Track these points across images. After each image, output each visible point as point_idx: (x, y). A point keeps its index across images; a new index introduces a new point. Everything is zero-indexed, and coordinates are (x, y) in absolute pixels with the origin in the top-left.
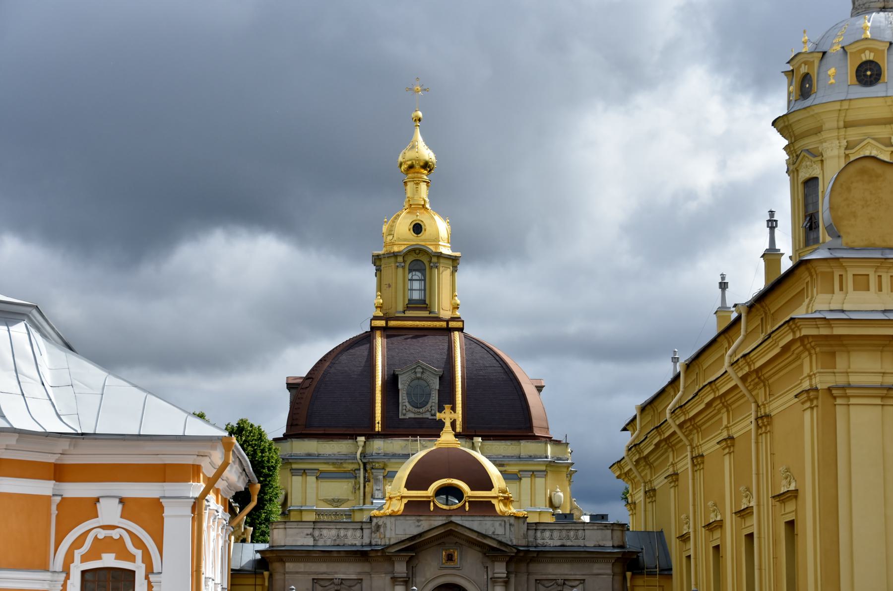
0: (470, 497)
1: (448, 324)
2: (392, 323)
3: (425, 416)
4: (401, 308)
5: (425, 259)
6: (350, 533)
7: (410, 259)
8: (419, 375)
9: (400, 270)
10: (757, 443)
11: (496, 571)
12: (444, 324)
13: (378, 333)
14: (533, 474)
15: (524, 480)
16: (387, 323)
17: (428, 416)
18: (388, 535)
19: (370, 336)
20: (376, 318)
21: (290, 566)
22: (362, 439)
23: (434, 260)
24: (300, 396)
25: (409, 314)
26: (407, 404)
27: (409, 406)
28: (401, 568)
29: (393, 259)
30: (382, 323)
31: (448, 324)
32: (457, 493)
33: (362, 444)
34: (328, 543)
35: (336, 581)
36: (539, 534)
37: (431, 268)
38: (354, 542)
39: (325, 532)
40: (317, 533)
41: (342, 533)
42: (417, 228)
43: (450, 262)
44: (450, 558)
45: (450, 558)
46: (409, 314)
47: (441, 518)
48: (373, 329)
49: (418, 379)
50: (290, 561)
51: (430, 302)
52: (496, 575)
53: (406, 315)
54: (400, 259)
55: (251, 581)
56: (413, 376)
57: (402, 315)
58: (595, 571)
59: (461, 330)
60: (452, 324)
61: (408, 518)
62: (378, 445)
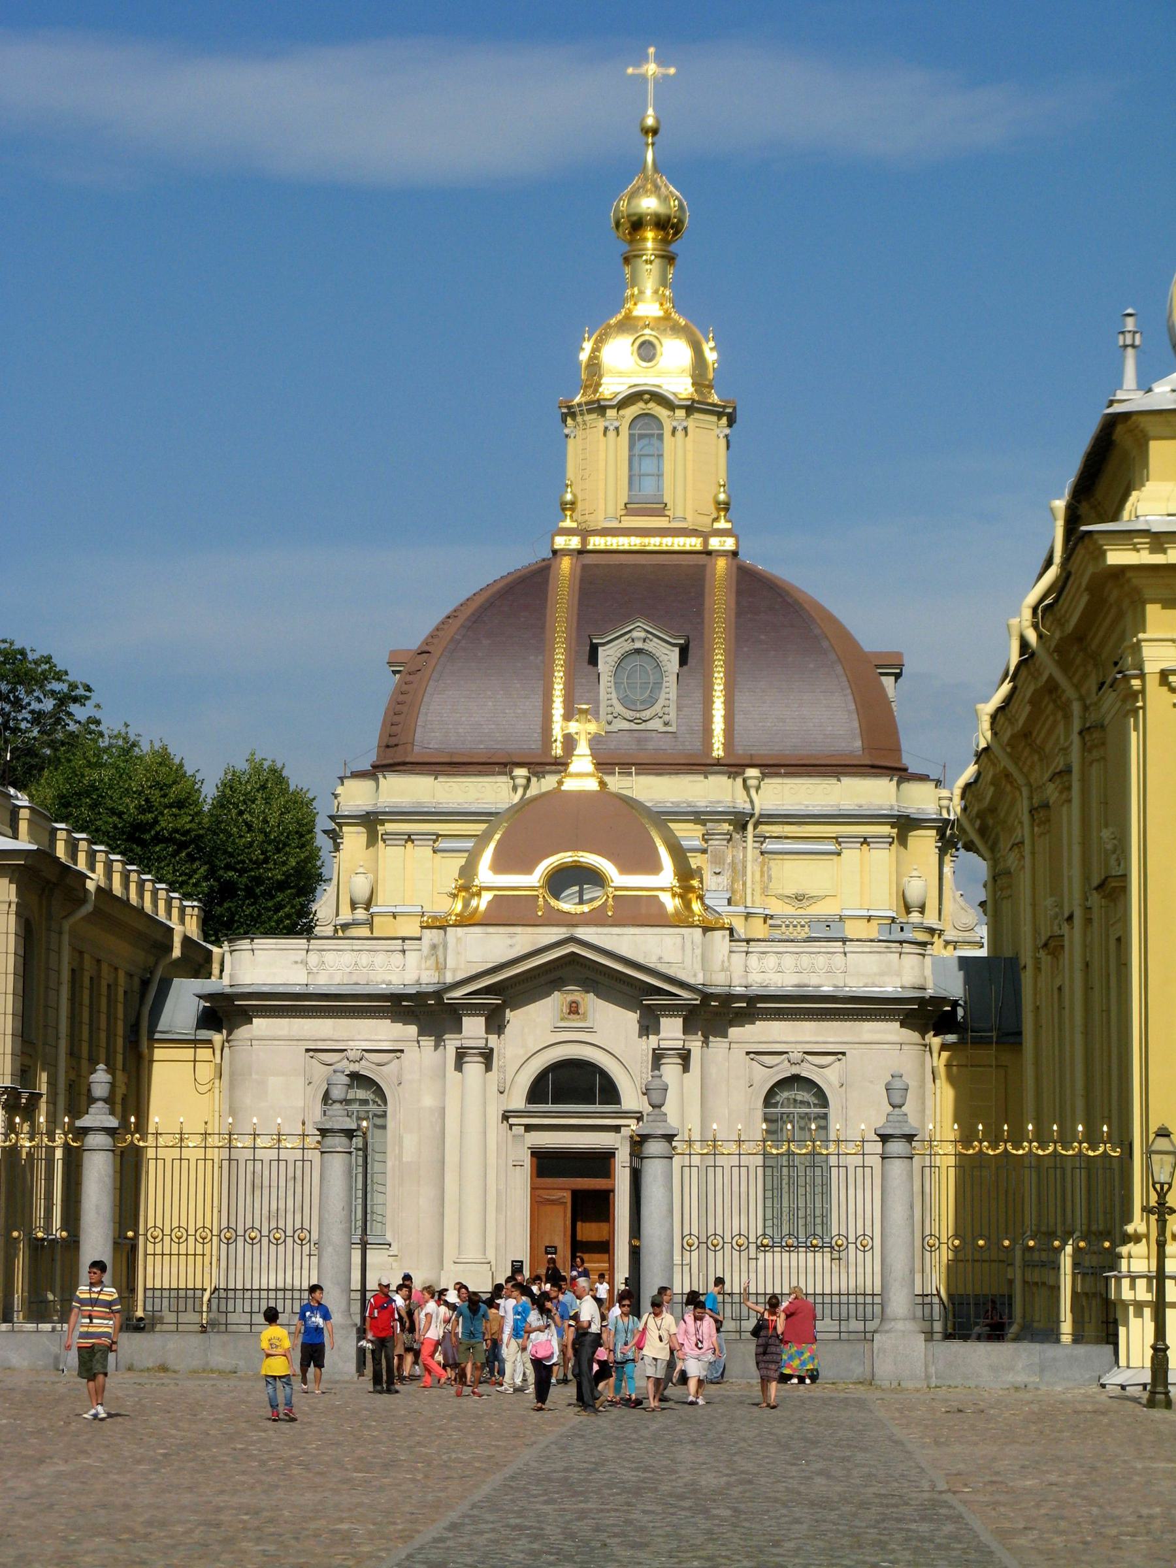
0: (617, 888)
1: (706, 543)
2: (596, 542)
3: (650, 725)
6: (380, 959)
8: (638, 645)
10: (1084, 780)
11: (663, 1035)
14: (865, 841)
16: (584, 542)
17: (656, 724)
18: (450, 963)
19: (548, 567)
21: (260, 1025)
23: (681, 413)
24: (405, 688)
26: (615, 702)
27: (619, 708)
28: (474, 1027)
30: (575, 543)
31: (706, 543)
32: (595, 878)
34: (337, 980)
35: (350, 1054)
36: (753, 960)
38: (388, 978)
39: (329, 957)
40: (313, 958)
41: (364, 959)
44: (574, 1009)
45: (574, 1009)
47: (555, 930)
49: (639, 651)
50: (260, 1017)
52: (664, 1044)
53: (624, 525)
55: (188, 1053)
56: (629, 646)
57: (615, 524)
58: (867, 1037)
61: (491, 929)
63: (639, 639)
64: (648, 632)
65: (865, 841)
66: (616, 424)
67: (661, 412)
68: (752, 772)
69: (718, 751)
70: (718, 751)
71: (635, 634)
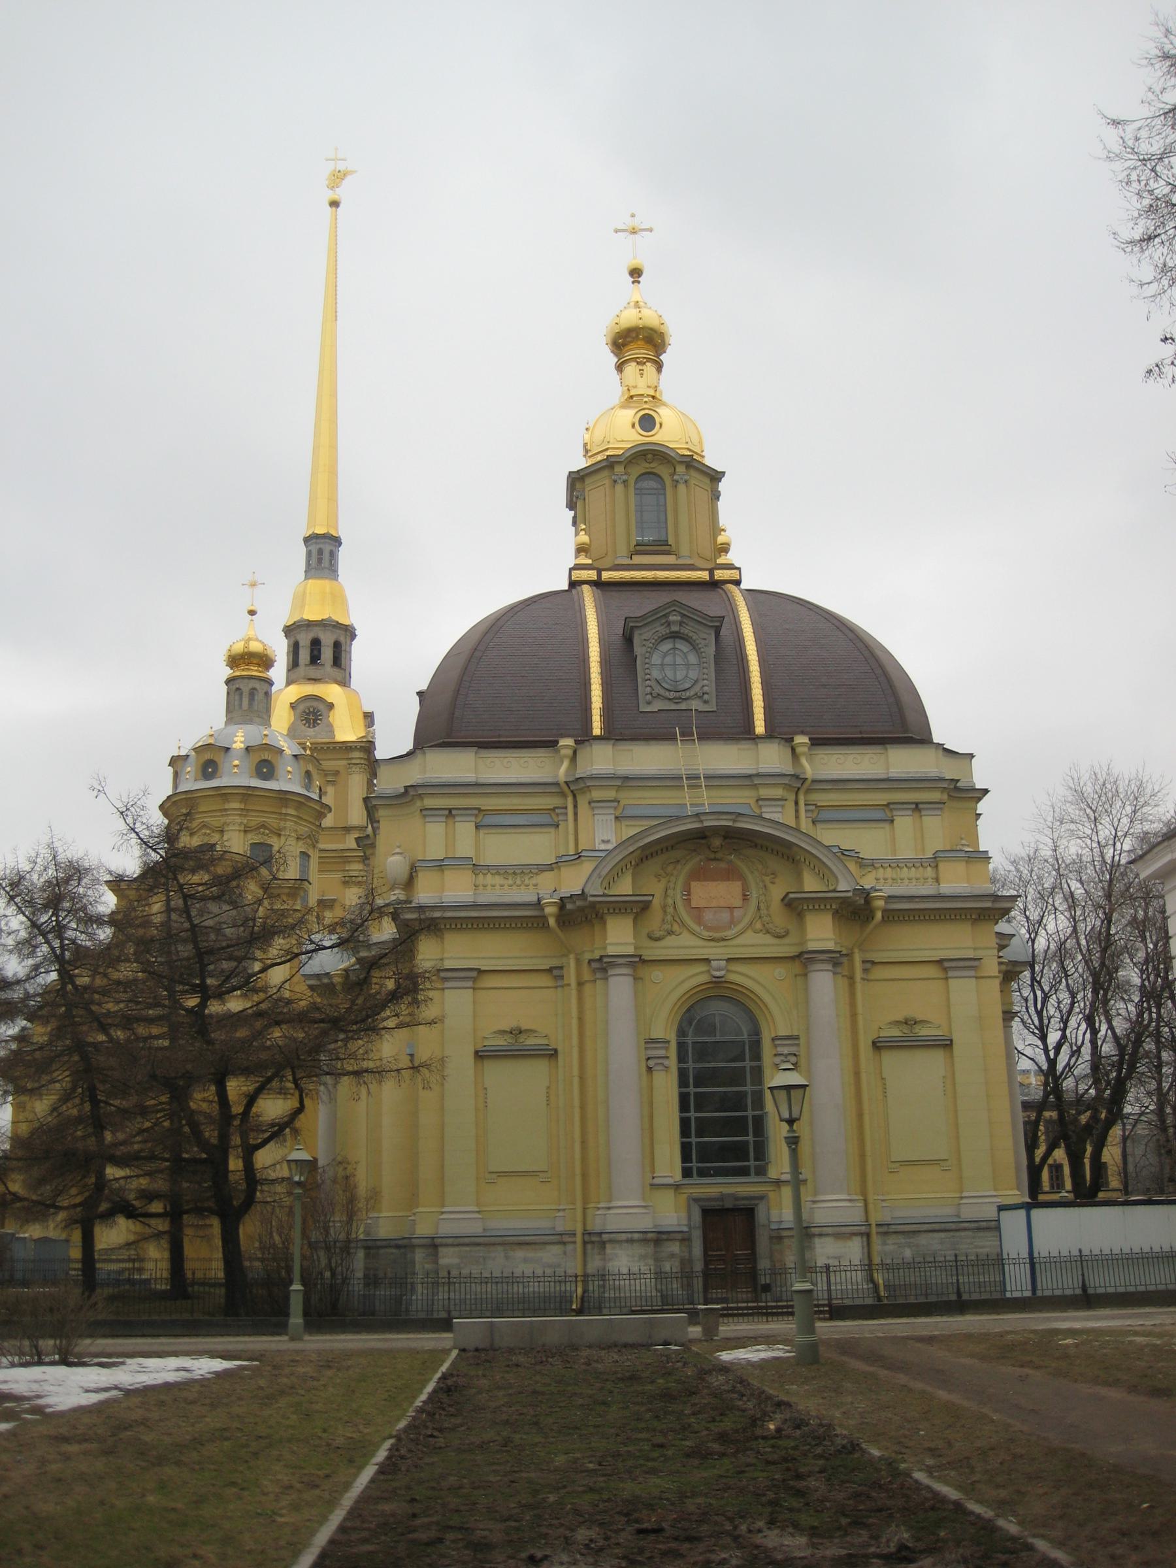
1: (711, 572)
4: (622, 550)
5: (664, 471)
7: (635, 471)
8: (675, 628)
9: (619, 488)
12: (704, 575)
13: (586, 588)
15: (898, 821)
16: (599, 575)
20: (577, 567)
22: (569, 742)
23: (681, 469)
25: (637, 559)
29: (606, 473)
30: (592, 575)
31: (711, 572)
33: (570, 752)
37: (676, 483)
42: (647, 422)
43: (707, 481)
46: (637, 559)
48: (573, 584)
51: (677, 542)
54: (619, 469)
56: (663, 630)
57: (628, 561)
59: (737, 583)
60: (719, 575)
62: (602, 759)
63: (674, 622)
64: (683, 615)
65: (917, 807)
66: (624, 477)
67: (664, 471)
68: (801, 739)
69: (760, 728)
70: (760, 728)
71: (672, 618)
